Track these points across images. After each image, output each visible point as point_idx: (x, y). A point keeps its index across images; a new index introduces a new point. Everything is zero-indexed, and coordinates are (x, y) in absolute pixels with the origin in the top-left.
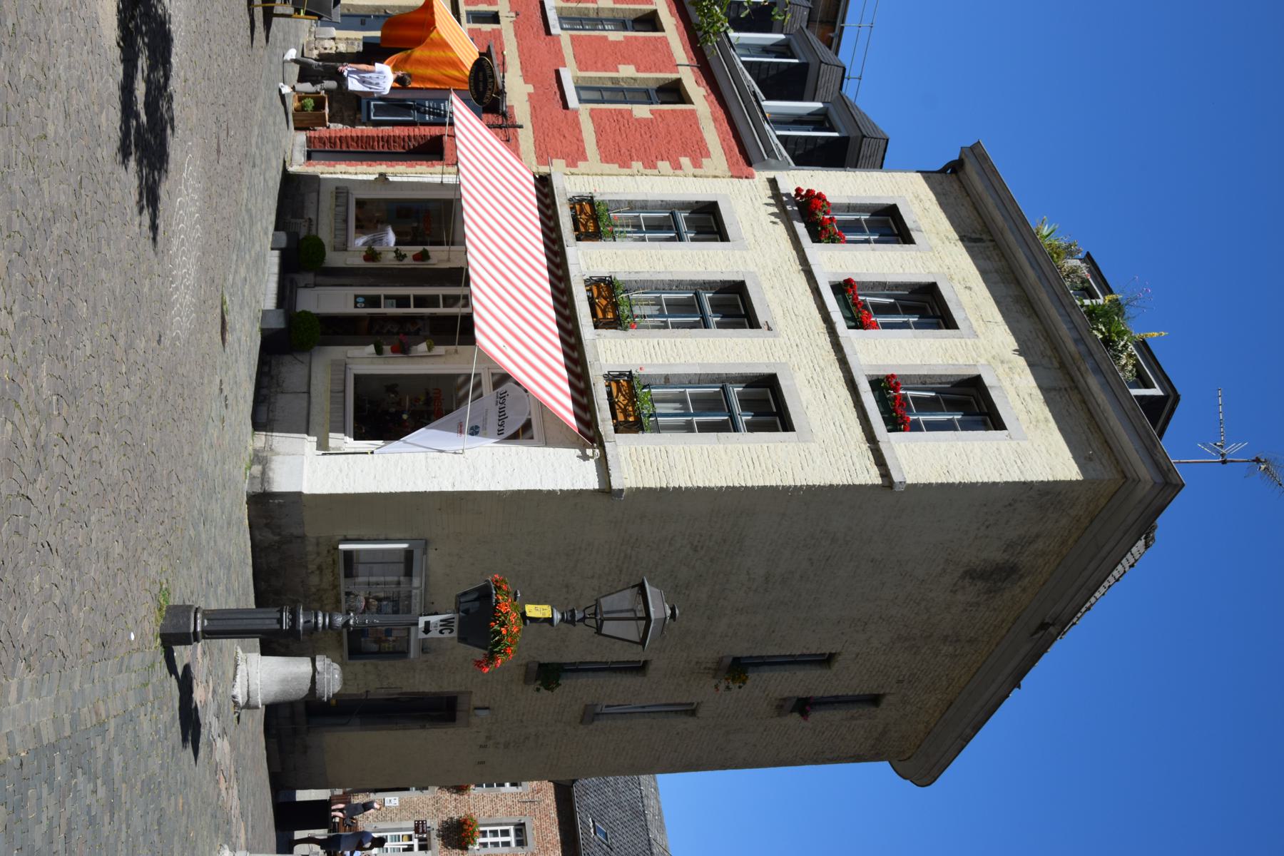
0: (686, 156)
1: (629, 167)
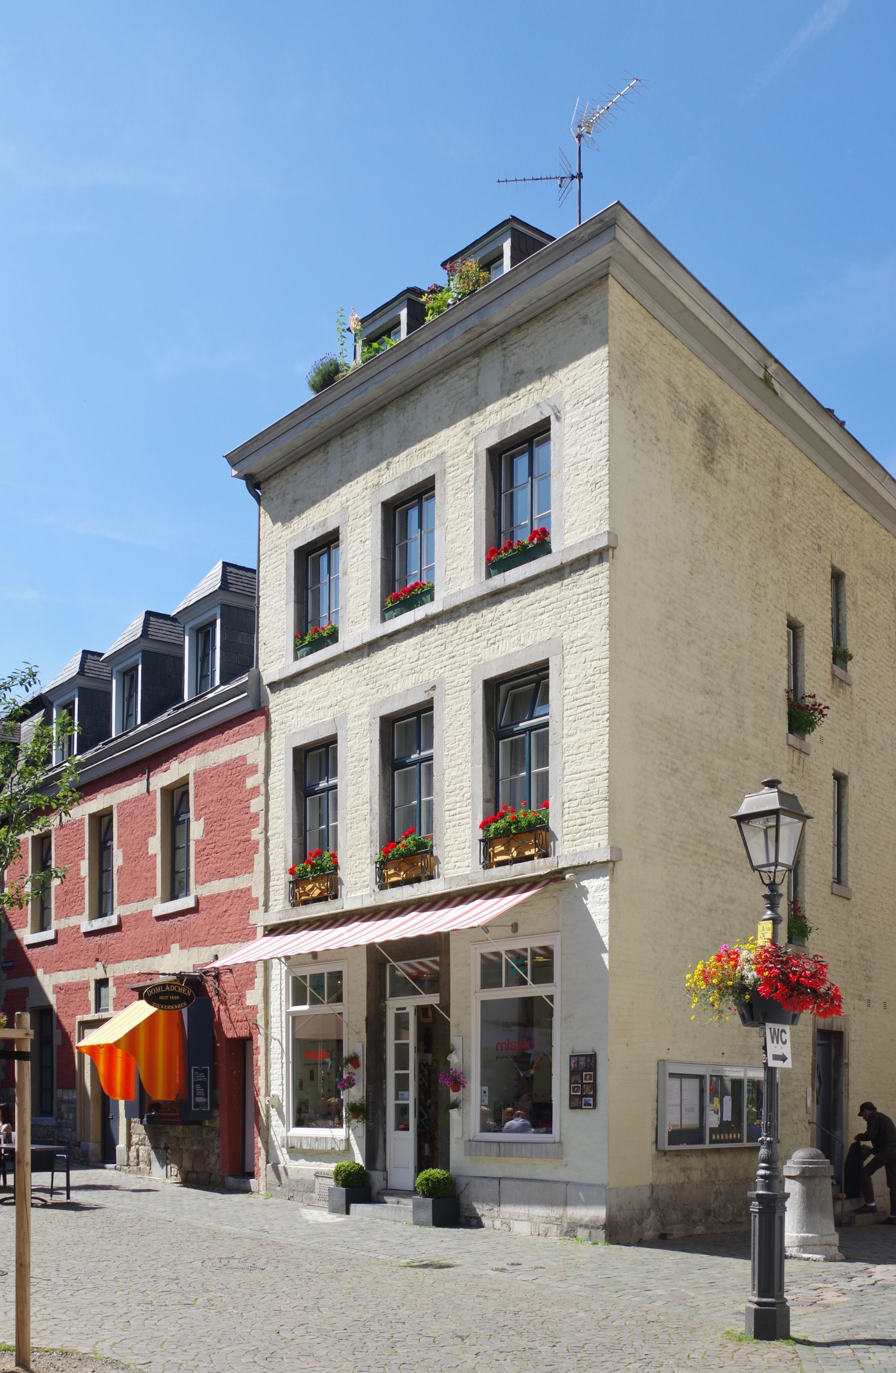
0: (244, 782)
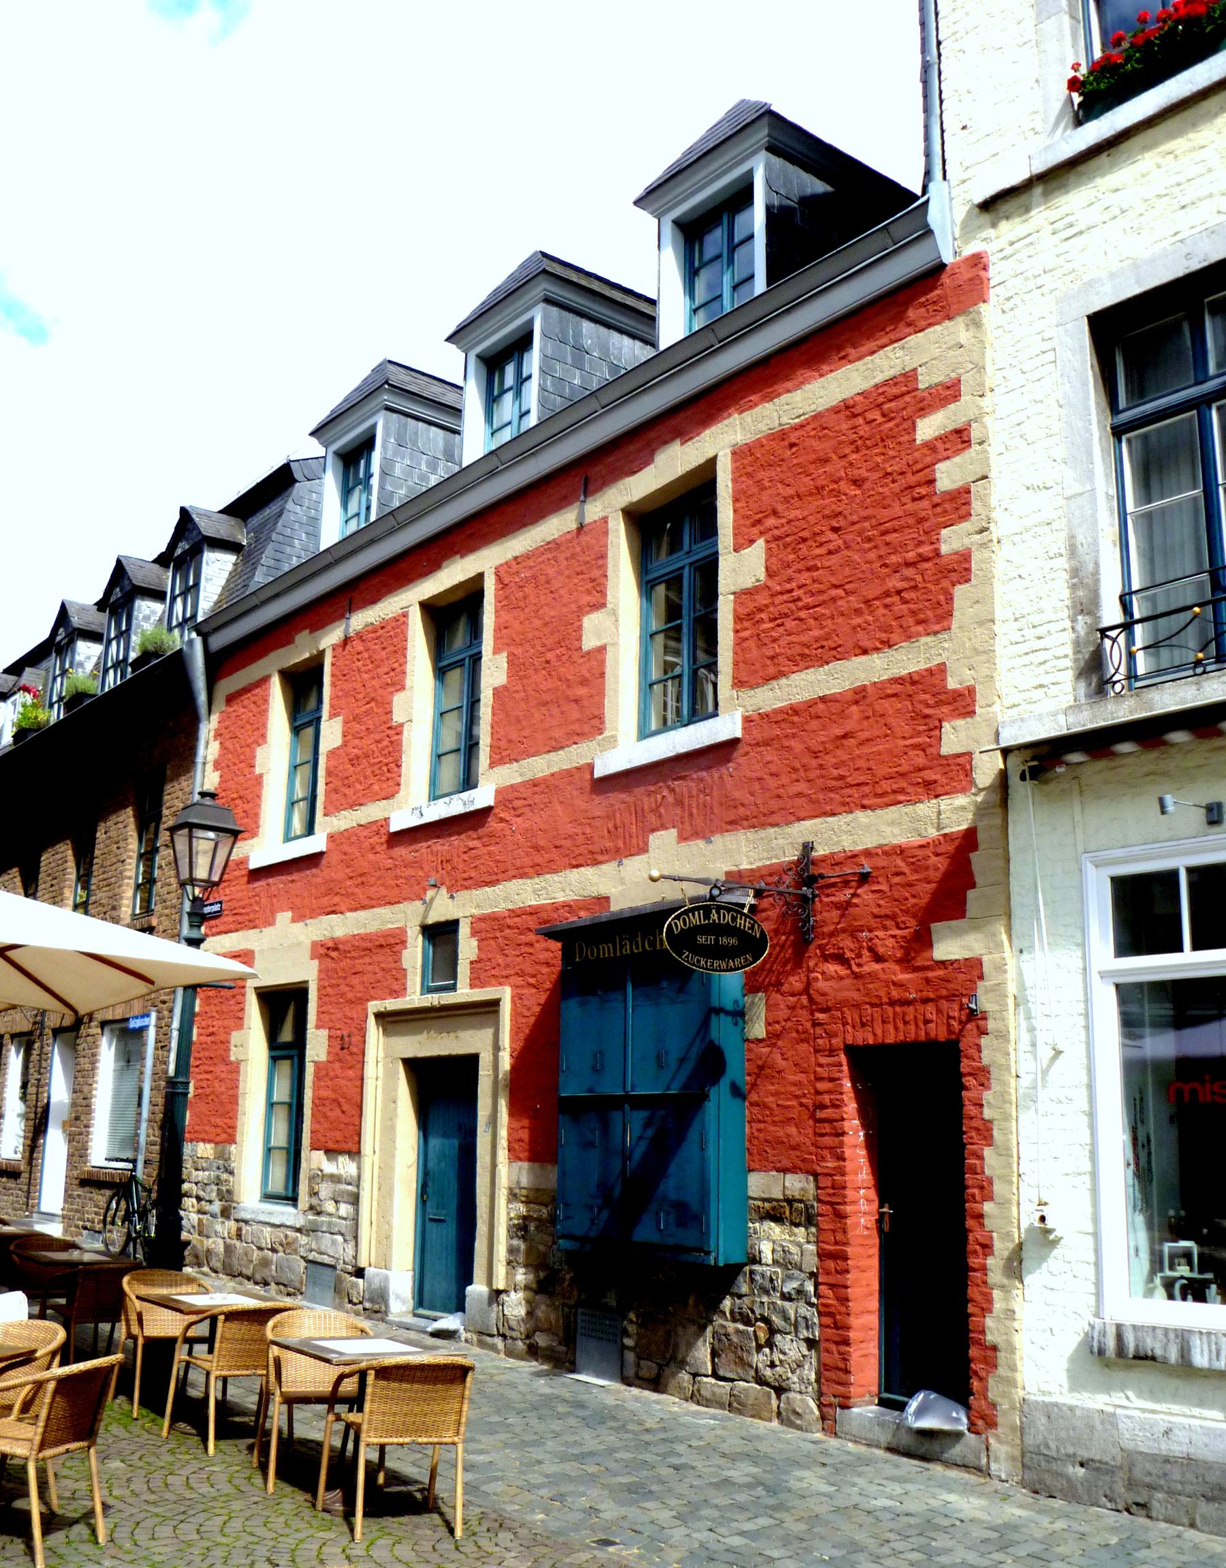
0: (914, 427)
1: (964, 557)
